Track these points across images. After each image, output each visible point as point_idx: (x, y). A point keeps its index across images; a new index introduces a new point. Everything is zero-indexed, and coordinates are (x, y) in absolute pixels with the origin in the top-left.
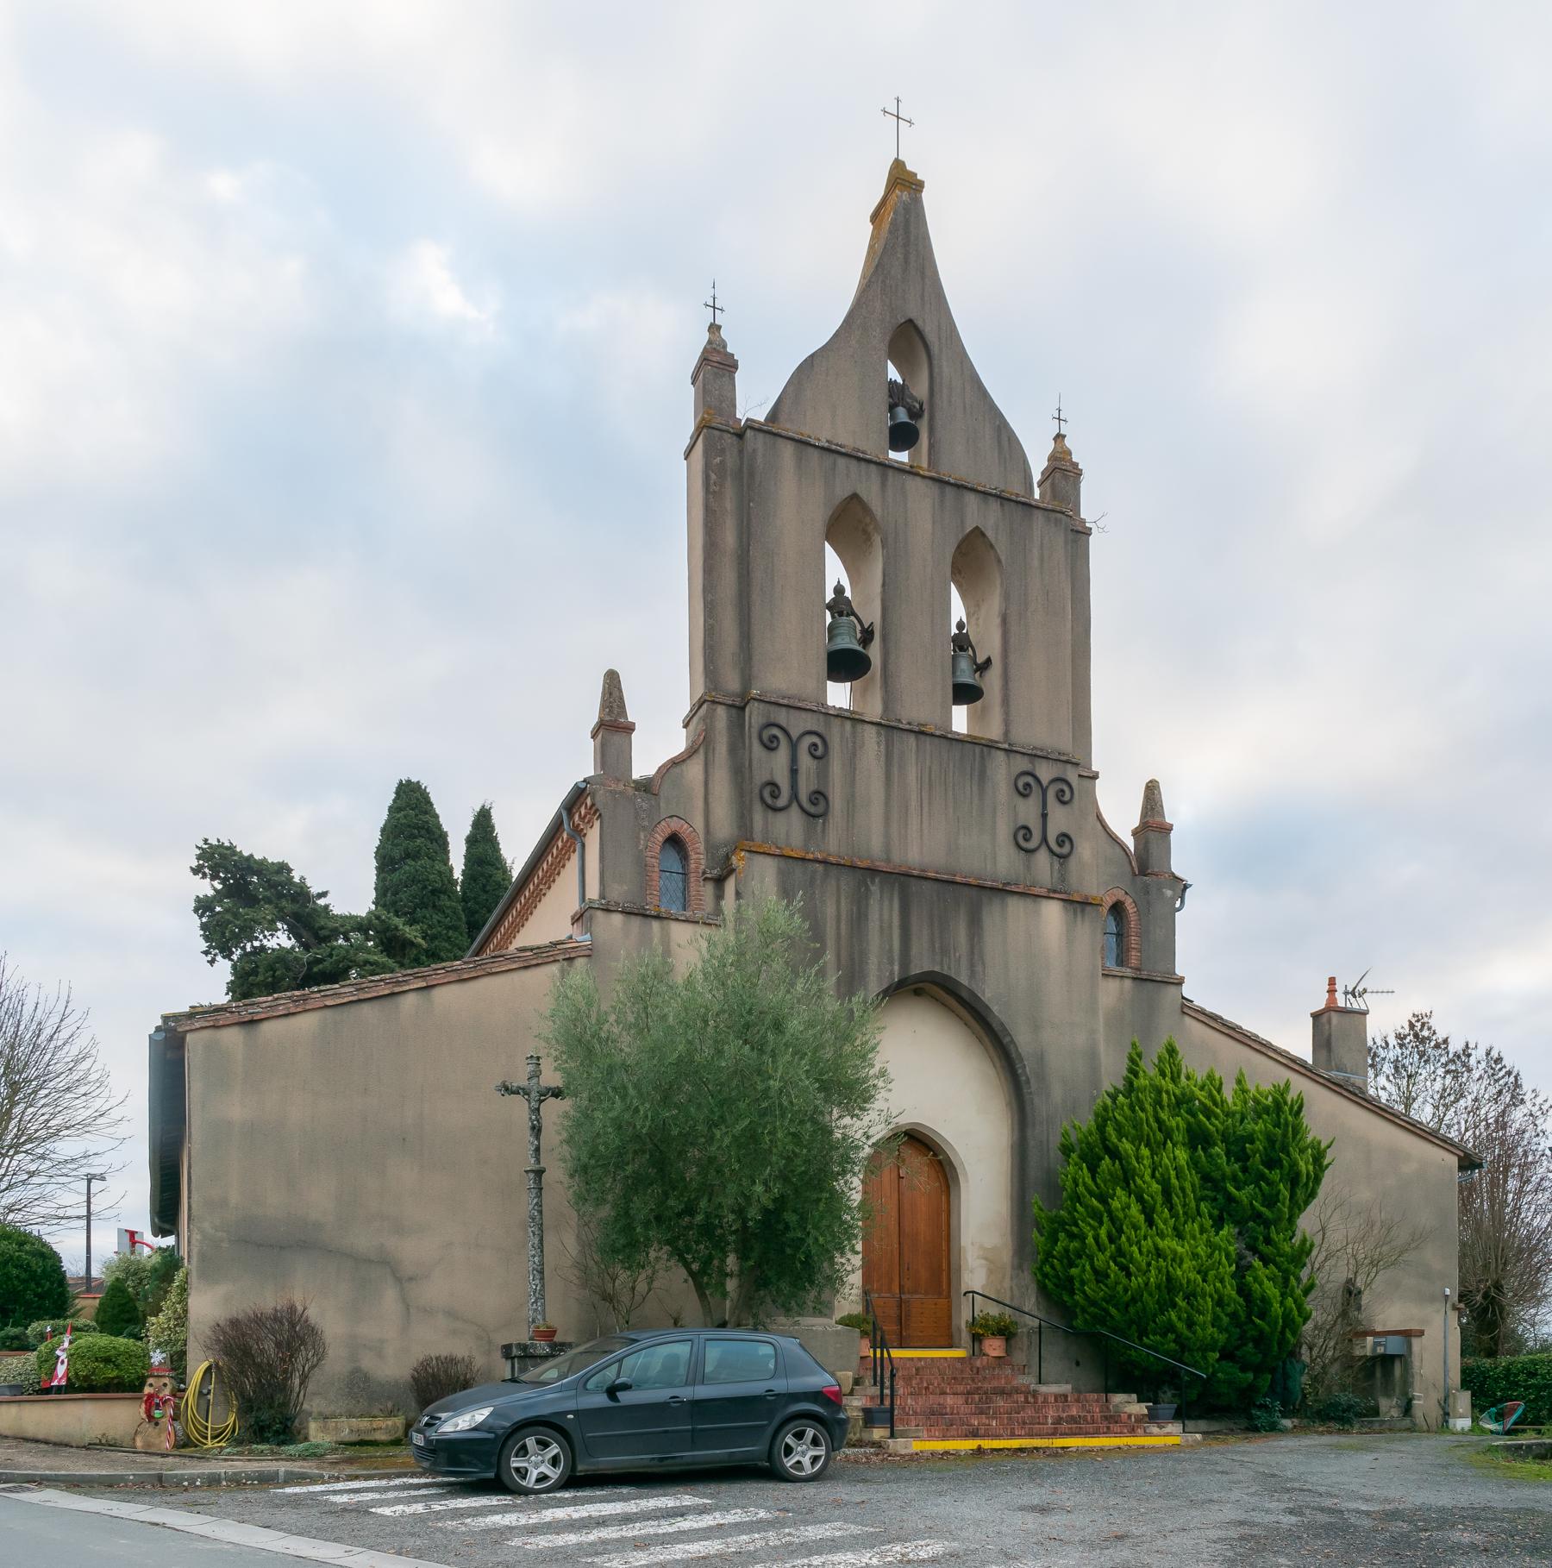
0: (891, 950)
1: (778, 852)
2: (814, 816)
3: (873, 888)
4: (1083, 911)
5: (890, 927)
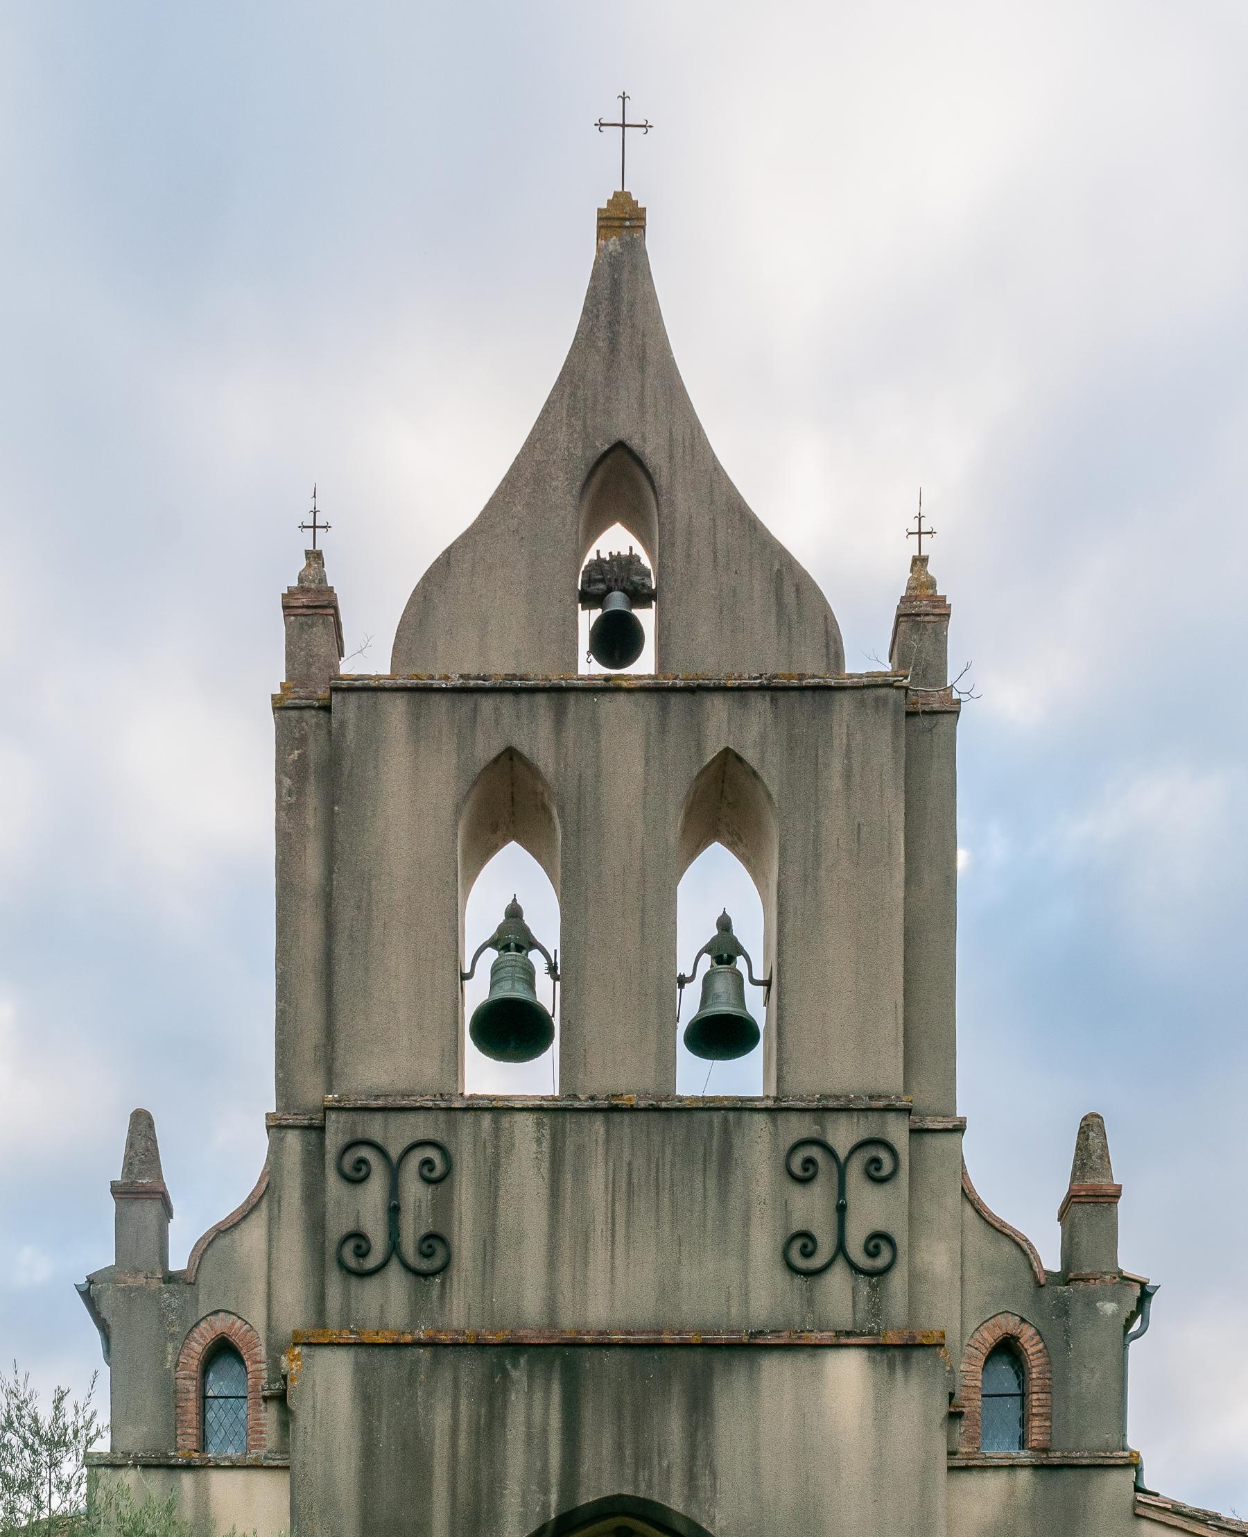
0: (545, 1469)
1: (353, 1338)
2: (426, 1275)
3: (515, 1374)
4: (907, 1360)
5: (545, 1431)
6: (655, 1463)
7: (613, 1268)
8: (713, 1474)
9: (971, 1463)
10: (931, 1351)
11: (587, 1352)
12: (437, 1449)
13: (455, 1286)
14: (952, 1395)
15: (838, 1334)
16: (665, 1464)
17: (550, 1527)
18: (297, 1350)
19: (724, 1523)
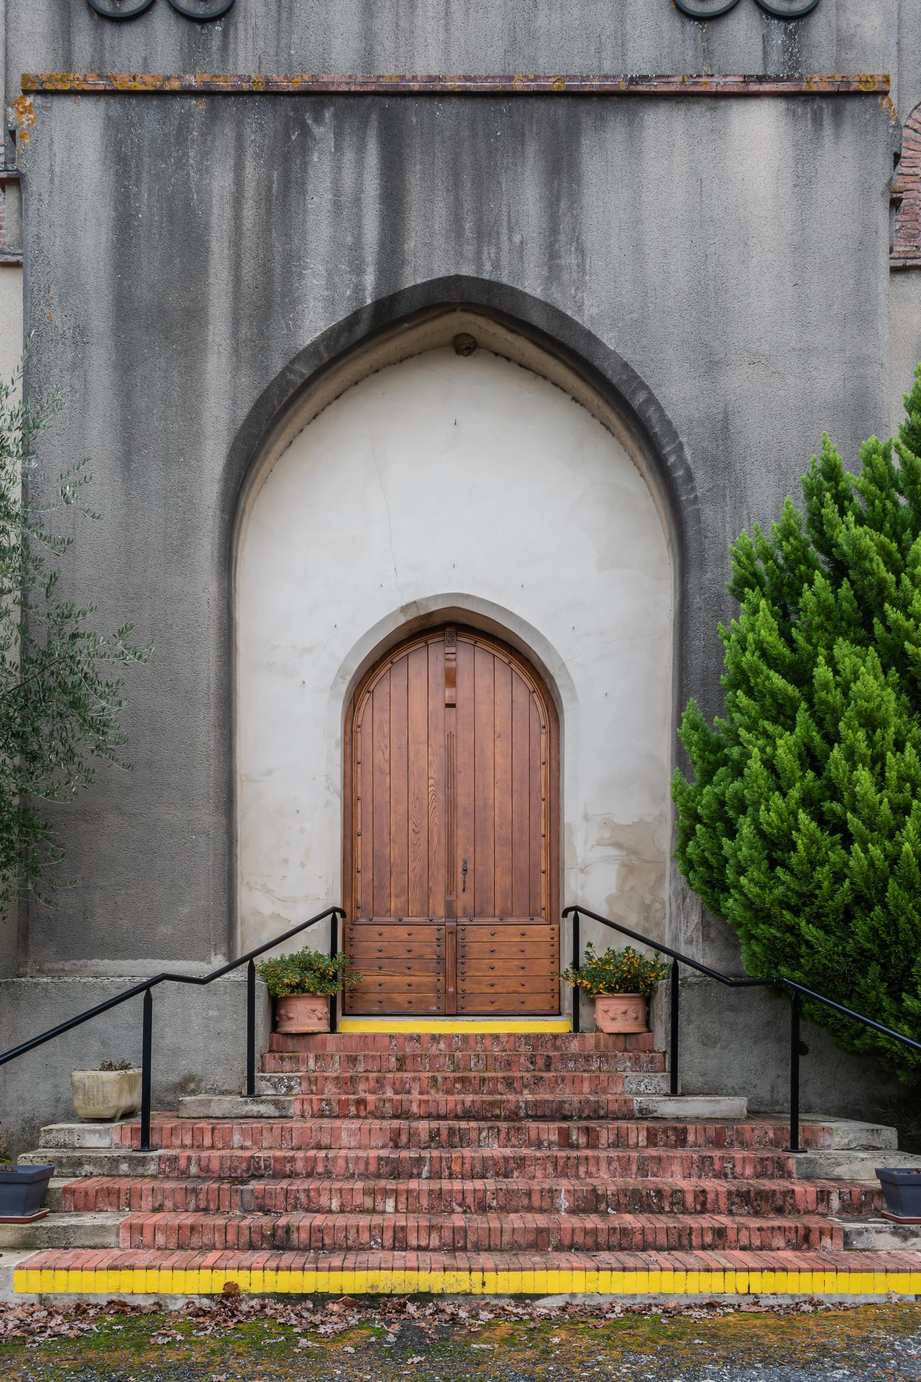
0: (358, 245)
1: (101, 85)
2: (203, 21)
3: (318, 131)
4: (838, 115)
5: (357, 201)
6: (504, 237)
7: (447, 13)
8: (581, 251)
9: (910, 263)
10: (869, 101)
11: (413, 105)
12: (214, 221)
13: (241, 34)
14: (897, 157)
15: (747, 79)
16: (517, 239)
17: (365, 316)
18: (29, 100)
19: (595, 310)
